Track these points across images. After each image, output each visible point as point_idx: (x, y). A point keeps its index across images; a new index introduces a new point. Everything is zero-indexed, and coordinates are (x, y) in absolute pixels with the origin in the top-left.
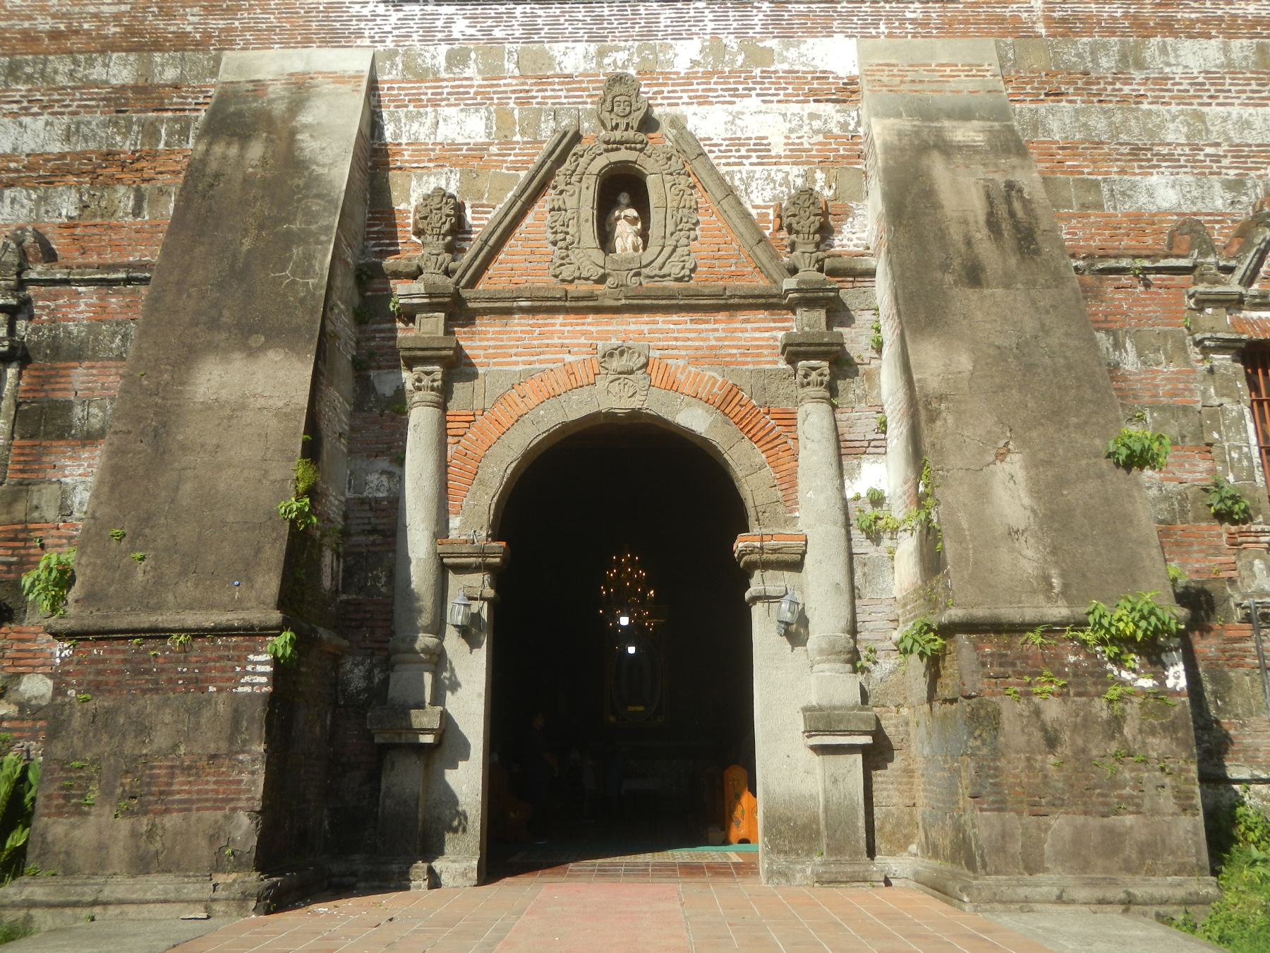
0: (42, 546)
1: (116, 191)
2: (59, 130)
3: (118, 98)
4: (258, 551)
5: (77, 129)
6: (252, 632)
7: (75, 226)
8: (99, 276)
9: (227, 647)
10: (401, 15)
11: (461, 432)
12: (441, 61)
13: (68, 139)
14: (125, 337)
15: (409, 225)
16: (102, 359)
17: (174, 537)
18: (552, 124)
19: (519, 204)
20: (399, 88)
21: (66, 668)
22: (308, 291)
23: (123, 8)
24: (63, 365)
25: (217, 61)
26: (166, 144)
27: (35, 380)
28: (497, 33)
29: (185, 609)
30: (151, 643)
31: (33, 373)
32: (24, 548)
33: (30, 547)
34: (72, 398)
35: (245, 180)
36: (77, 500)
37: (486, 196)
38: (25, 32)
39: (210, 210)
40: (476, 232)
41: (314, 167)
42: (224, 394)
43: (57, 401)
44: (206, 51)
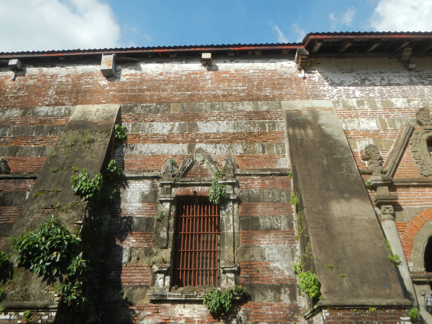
0: (258, 272)
1: (255, 145)
2: (231, 125)
3: (249, 115)
4: (387, 274)
5: (238, 125)
6: (400, 307)
7: (243, 157)
8: (261, 173)
9: (391, 314)
10: (337, 90)
11: (403, 230)
12: (355, 104)
13: (235, 128)
14: (273, 194)
15: (359, 157)
16: (267, 202)
17: (352, 268)
18: (400, 124)
19: (402, 150)
20: (343, 112)
21: (329, 321)
22: (355, 178)
23: (245, 88)
24: (253, 204)
25: (280, 105)
26: (269, 130)
27: (244, 209)
28: (371, 95)
29: (369, 297)
30: (360, 312)
31: (243, 206)
32: (251, 271)
33: (253, 271)
34: (258, 216)
35: (312, 141)
36: (267, 253)
37: (384, 147)
38: (213, 95)
39: (306, 151)
40: (385, 159)
41: (333, 137)
42: (345, 214)
43: (253, 217)
44: (275, 101)
